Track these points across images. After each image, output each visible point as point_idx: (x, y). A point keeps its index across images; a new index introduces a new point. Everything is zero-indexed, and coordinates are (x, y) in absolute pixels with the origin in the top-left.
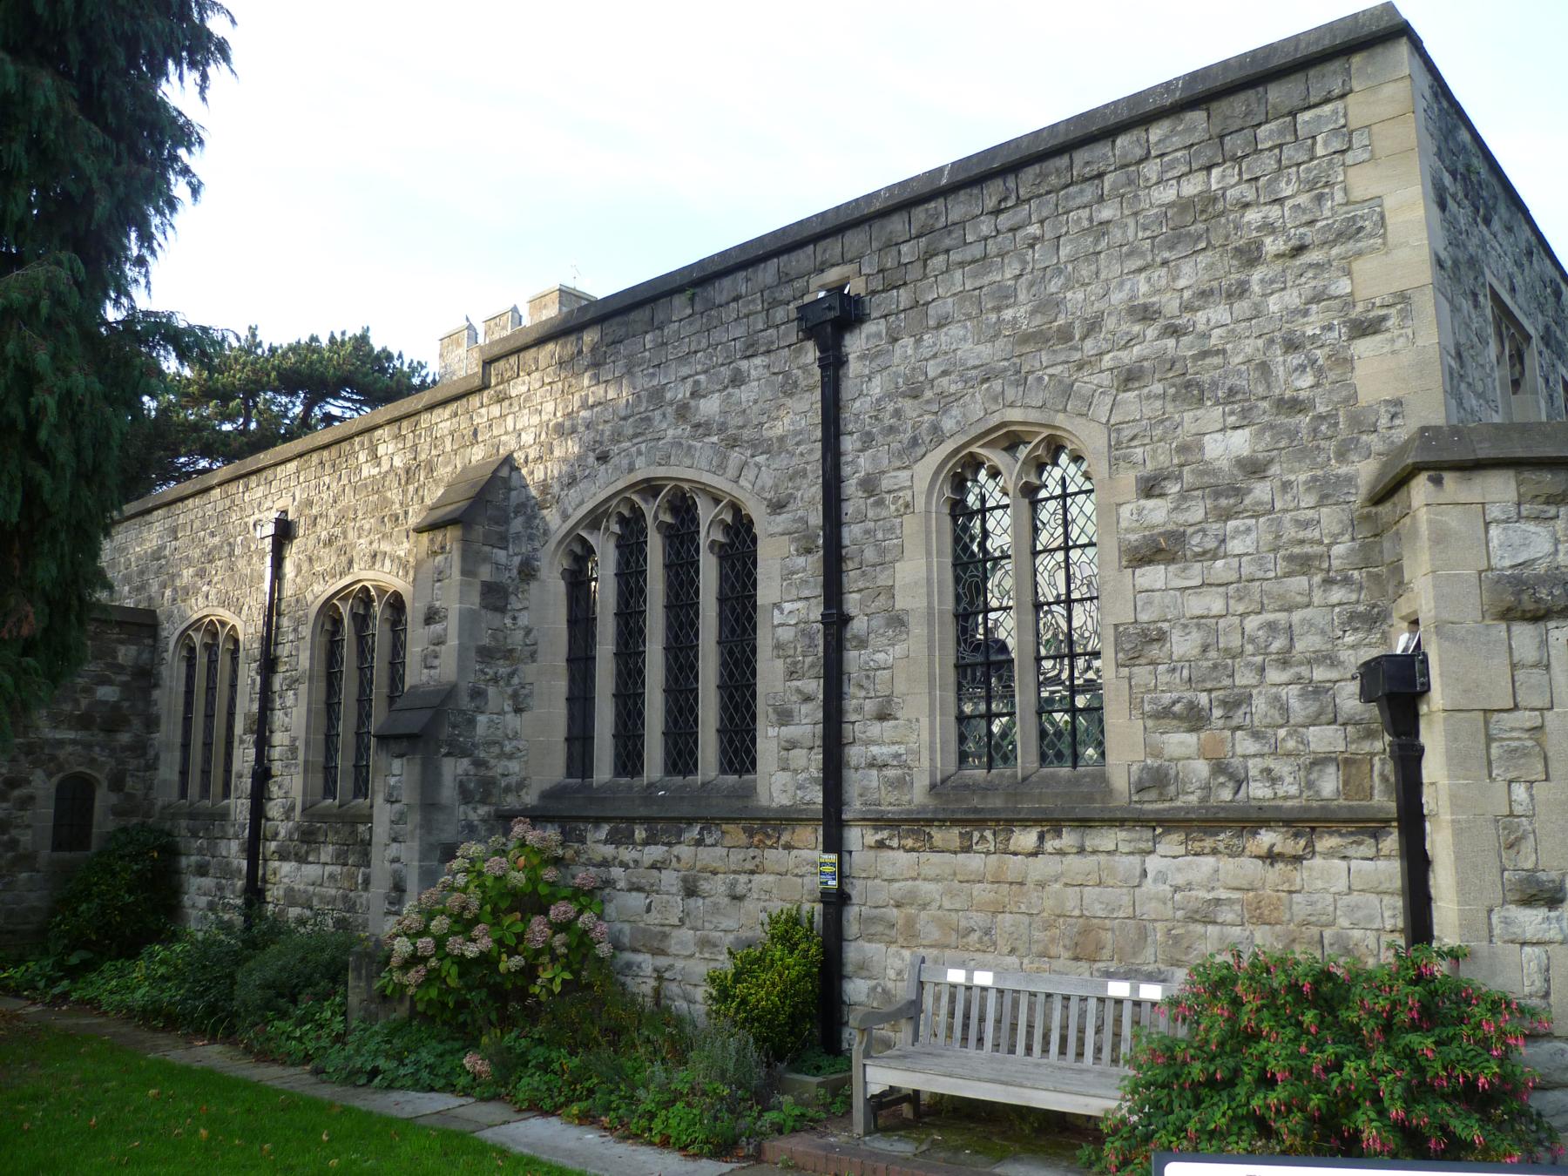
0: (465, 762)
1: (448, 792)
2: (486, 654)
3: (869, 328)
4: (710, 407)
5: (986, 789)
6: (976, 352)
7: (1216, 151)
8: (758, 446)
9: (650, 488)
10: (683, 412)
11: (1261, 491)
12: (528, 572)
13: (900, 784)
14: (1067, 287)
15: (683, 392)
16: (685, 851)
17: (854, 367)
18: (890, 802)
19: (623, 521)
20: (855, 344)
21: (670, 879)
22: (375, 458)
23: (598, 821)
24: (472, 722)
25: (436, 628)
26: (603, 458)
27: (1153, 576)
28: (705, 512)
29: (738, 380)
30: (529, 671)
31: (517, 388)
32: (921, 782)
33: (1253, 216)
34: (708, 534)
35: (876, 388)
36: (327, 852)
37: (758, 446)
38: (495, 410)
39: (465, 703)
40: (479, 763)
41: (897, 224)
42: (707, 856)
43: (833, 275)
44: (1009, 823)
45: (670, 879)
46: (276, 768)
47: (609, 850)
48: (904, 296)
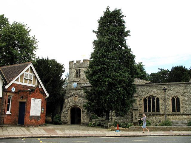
4: (156, 92)
7: (186, 86)
9: (151, 96)
11: (188, 101)
15: (154, 91)
27: (183, 104)
29: (158, 91)
37: (160, 95)
48: (169, 89)
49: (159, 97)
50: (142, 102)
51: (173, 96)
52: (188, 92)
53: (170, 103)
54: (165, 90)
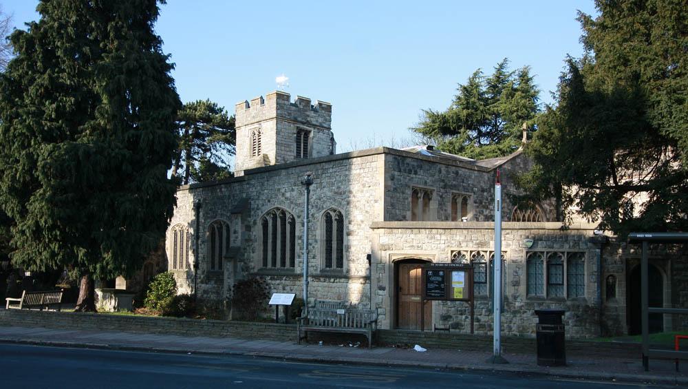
0: (242, 263)
1: (239, 269)
2: (247, 241)
3: (313, 185)
4: (288, 195)
5: (328, 271)
6: (329, 194)
8: (296, 204)
10: (283, 195)
12: (255, 223)
13: (316, 270)
14: (342, 184)
15: (283, 191)
16: (283, 281)
17: (311, 193)
18: (314, 273)
19: (273, 214)
20: (311, 188)
21: (281, 286)
22: (221, 191)
23: (268, 275)
24: (244, 255)
25: (237, 235)
26: (269, 201)
28: (288, 216)
29: (293, 190)
30: (256, 244)
31: (253, 182)
32: (319, 270)
33: (365, 179)
34: (288, 220)
35: (314, 197)
36: (213, 282)
37: (296, 204)
38: (248, 186)
39: (242, 251)
40: (245, 263)
41: (318, 166)
42: (287, 283)
43: (308, 173)
44: (330, 277)
45: (281, 286)
46: (200, 262)
47: (270, 281)
49: (295, 212)
50: (257, 231)
51: (328, 205)
52: (365, 189)
53: (320, 232)
54: (308, 184)
